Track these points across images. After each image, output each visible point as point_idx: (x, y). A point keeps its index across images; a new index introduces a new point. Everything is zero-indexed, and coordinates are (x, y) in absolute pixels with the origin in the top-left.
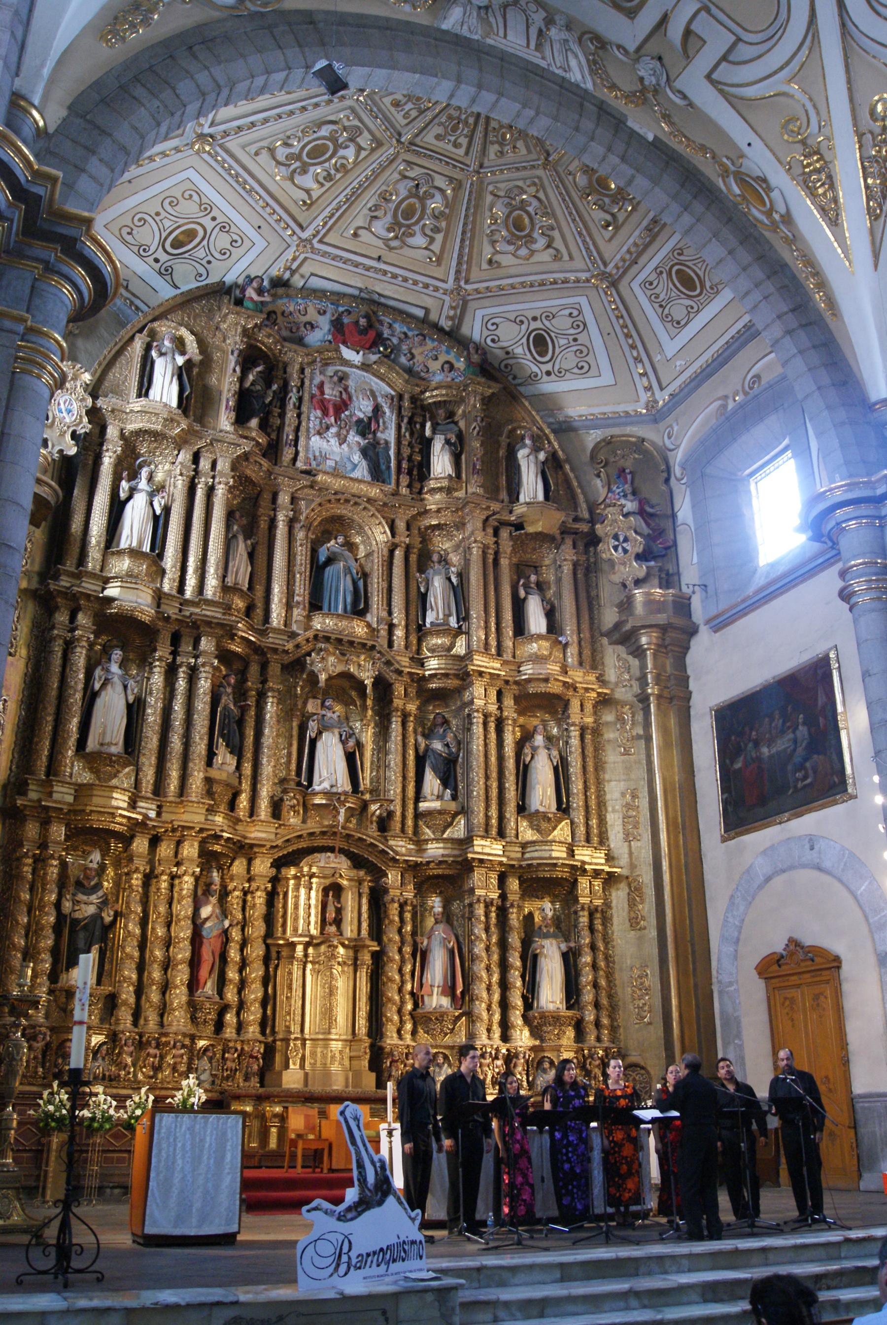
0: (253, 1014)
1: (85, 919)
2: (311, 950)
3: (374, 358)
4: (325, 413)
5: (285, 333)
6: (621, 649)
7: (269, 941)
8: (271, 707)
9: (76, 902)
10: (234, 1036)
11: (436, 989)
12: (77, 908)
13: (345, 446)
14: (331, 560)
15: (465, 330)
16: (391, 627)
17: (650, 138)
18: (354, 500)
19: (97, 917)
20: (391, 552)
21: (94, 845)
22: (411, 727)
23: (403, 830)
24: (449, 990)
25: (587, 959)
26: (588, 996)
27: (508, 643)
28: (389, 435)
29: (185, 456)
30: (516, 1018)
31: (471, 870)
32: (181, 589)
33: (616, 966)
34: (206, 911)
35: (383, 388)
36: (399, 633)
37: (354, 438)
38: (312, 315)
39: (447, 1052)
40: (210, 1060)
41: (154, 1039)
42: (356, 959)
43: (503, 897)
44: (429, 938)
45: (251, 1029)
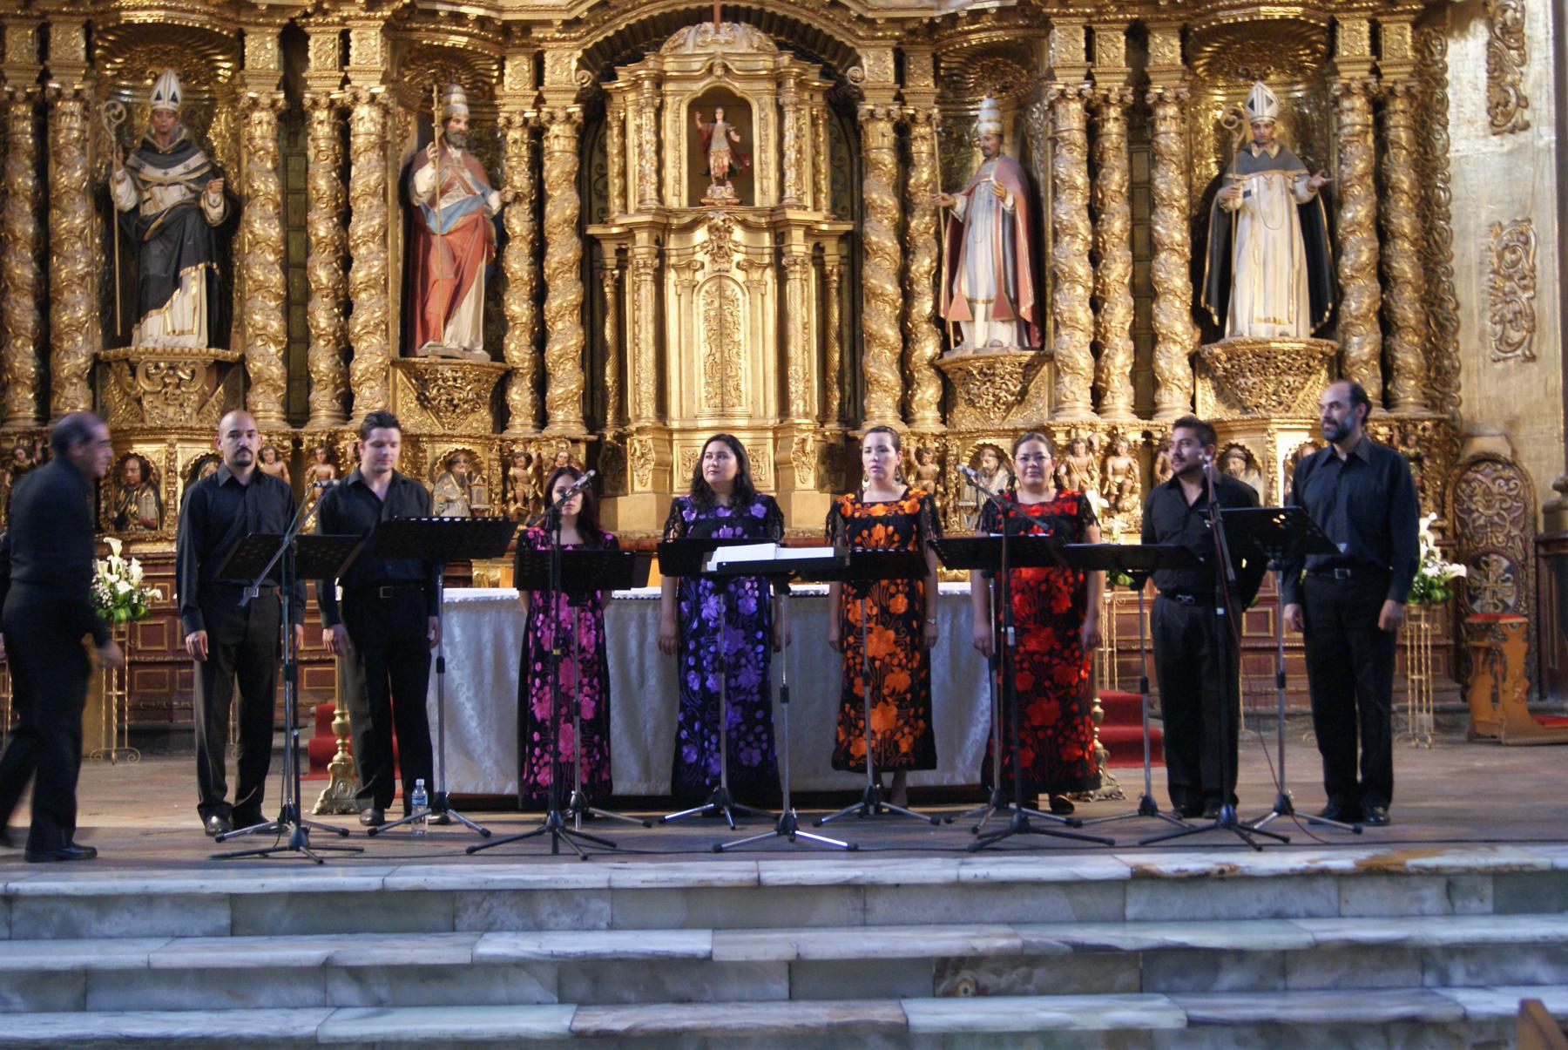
0: (566, 382)
1: (157, 216)
2: (672, 243)
7: (594, 230)
9: (141, 185)
10: (530, 432)
11: (980, 310)
12: (147, 195)
19: (191, 208)
21: (166, 61)
24: (1006, 307)
25: (1357, 212)
26: (1360, 299)
30: (1173, 362)
31: (1046, 25)
33: (1455, 226)
34: (424, 180)
39: (1005, 444)
40: (465, 482)
41: (321, 444)
42: (778, 253)
43: (1140, 81)
44: (969, 194)
45: (559, 415)
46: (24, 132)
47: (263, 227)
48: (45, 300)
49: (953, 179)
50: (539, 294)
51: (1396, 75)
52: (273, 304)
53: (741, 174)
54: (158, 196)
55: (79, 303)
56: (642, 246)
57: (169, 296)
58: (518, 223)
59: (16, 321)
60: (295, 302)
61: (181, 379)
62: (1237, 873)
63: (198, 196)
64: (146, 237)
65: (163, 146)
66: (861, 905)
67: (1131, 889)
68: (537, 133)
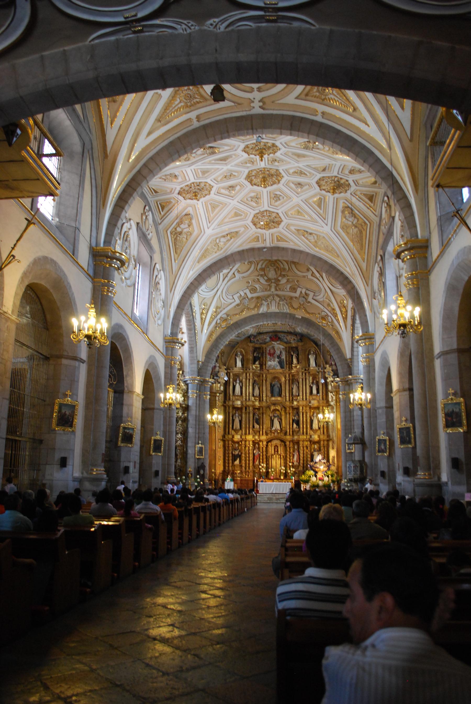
3: (278, 342)
4: (270, 356)
5: (261, 342)
6: (332, 394)
8: (264, 416)
13: (275, 362)
14: (274, 385)
15: (297, 331)
16: (286, 396)
17: (300, 317)
18: (277, 373)
20: (286, 381)
22: (291, 414)
23: (290, 434)
24: (297, 461)
27: (308, 397)
28: (283, 357)
29: (244, 374)
32: (246, 400)
34: (255, 452)
35: (282, 347)
36: (288, 398)
37: (277, 360)
38: (265, 337)
47: (243, 455)
48: (228, 460)
49: (294, 451)
50: (263, 460)
51: (325, 445)
53: (278, 451)
56: (270, 457)
58: (261, 454)
60: (246, 461)
68: (263, 448)
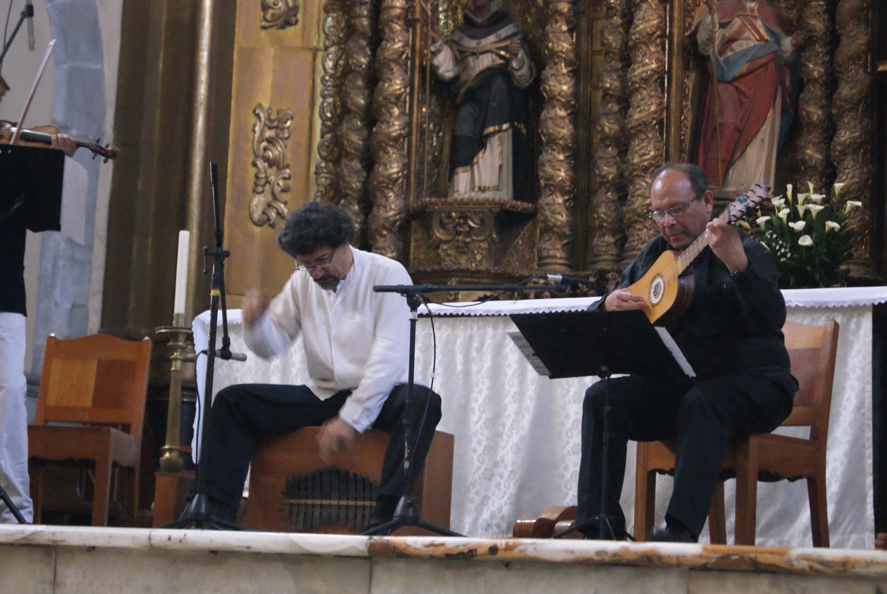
1: (466, 81)
9: (461, 57)
46: (361, 16)
52: (561, 157)
54: (472, 64)
55: (390, 162)
57: (474, 154)
58: (815, 69)
59: (344, 181)
61: (471, 227)
62: (516, 553)
63: (507, 61)
64: (458, 101)
65: (479, 20)
66: (49, 575)
67: (379, 572)
